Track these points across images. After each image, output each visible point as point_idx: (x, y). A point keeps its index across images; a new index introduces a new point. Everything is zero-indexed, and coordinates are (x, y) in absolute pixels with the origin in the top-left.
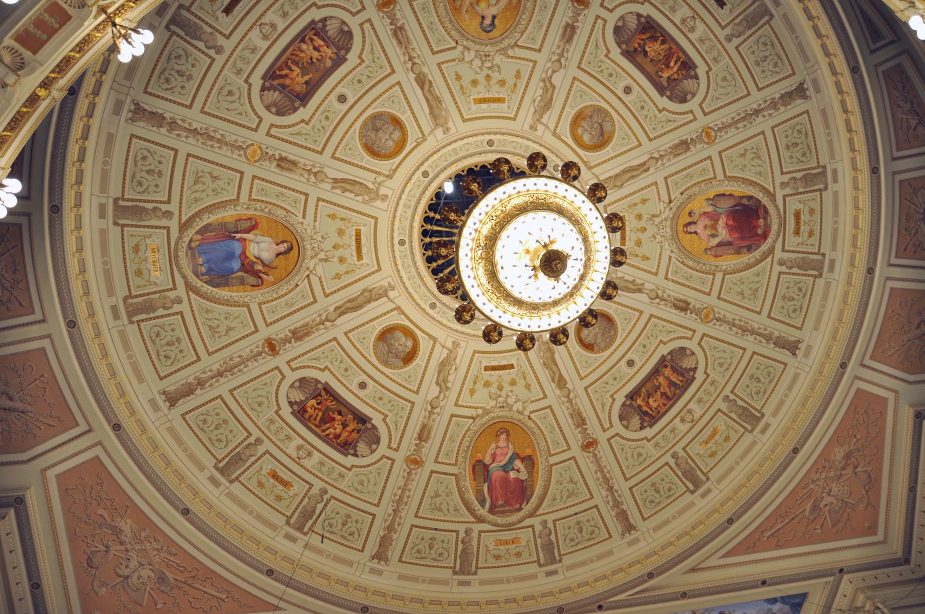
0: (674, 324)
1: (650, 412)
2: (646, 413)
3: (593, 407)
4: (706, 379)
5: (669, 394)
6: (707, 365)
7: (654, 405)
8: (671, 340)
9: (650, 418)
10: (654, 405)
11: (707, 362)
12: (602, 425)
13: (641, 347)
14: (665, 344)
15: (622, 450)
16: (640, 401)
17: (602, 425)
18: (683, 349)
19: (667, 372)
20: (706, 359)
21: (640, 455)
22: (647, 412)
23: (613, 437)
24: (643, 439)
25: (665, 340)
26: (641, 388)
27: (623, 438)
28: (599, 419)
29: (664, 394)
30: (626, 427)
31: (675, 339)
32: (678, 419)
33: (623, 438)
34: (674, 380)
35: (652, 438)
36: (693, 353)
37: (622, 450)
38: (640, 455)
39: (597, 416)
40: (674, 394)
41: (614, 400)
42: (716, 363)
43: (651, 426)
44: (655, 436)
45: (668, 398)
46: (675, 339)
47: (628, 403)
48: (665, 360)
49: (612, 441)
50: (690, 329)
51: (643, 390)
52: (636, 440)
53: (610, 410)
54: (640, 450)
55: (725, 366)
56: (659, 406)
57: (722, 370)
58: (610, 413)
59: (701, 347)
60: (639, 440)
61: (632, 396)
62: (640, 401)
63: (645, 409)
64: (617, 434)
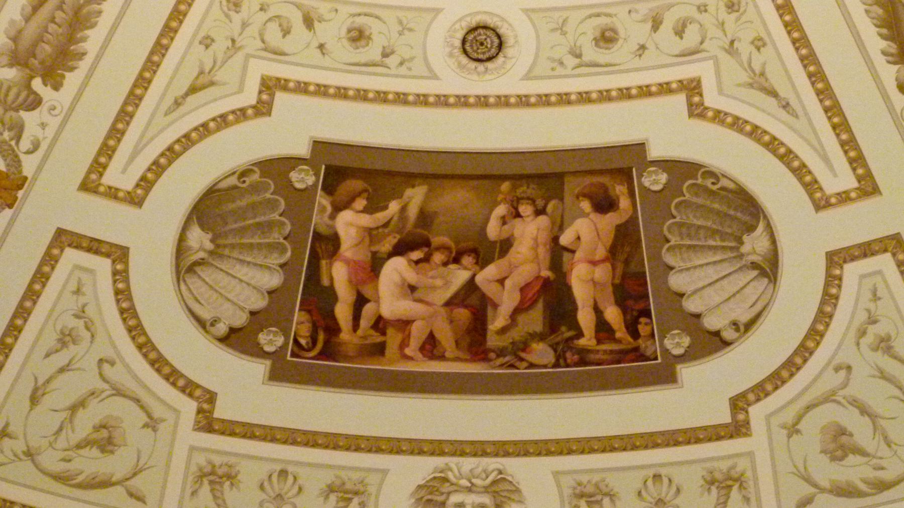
0: (817, 76)
1: (343, 312)
2: (319, 299)
3: (160, 48)
4: (714, 434)
5: (497, 322)
6: (777, 379)
7: (389, 301)
8: (737, 124)
9: (318, 335)
10: (389, 301)
11: (792, 366)
12: (107, 151)
13: (591, 28)
14: (697, 110)
15: (66, 339)
16: (350, 224)
17: (107, 151)
18: (746, 209)
19: (587, 230)
20: (804, 352)
21: (105, 440)
22: (331, 295)
23: (94, 246)
24: (189, 388)
25: (711, 99)
26: (411, 178)
27: (123, 295)
28: (125, 116)
29: (473, 303)
30: (185, 267)
31: (755, 133)
32: (424, 467)
33: (123, 295)
34: (581, 291)
35: (231, 429)
36: (769, 269)
37: (66, 339)
38: (105, 440)
39: (134, 99)
40: (519, 349)
41: (263, 109)
42: (827, 414)
43: (281, 373)
44: (249, 431)
45: (475, 342)
46: (755, 133)
47: (302, 178)
48: (624, 174)
49: (71, 257)
50: (857, 161)
51: (416, 196)
52: (158, 363)
53: (205, 130)
54: (129, 416)
55: (854, 471)
56: (404, 324)
57: (827, 472)
58: (187, 141)
59: (833, 281)
60: (172, 376)
61: (347, 172)
62: (350, 224)
63: (339, 275)
64: (119, 255)
